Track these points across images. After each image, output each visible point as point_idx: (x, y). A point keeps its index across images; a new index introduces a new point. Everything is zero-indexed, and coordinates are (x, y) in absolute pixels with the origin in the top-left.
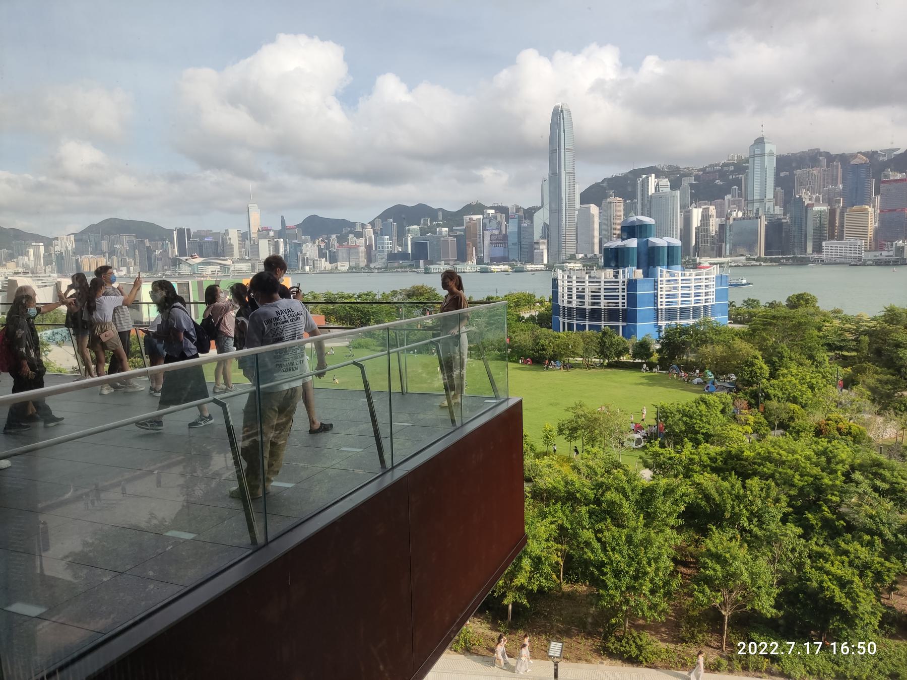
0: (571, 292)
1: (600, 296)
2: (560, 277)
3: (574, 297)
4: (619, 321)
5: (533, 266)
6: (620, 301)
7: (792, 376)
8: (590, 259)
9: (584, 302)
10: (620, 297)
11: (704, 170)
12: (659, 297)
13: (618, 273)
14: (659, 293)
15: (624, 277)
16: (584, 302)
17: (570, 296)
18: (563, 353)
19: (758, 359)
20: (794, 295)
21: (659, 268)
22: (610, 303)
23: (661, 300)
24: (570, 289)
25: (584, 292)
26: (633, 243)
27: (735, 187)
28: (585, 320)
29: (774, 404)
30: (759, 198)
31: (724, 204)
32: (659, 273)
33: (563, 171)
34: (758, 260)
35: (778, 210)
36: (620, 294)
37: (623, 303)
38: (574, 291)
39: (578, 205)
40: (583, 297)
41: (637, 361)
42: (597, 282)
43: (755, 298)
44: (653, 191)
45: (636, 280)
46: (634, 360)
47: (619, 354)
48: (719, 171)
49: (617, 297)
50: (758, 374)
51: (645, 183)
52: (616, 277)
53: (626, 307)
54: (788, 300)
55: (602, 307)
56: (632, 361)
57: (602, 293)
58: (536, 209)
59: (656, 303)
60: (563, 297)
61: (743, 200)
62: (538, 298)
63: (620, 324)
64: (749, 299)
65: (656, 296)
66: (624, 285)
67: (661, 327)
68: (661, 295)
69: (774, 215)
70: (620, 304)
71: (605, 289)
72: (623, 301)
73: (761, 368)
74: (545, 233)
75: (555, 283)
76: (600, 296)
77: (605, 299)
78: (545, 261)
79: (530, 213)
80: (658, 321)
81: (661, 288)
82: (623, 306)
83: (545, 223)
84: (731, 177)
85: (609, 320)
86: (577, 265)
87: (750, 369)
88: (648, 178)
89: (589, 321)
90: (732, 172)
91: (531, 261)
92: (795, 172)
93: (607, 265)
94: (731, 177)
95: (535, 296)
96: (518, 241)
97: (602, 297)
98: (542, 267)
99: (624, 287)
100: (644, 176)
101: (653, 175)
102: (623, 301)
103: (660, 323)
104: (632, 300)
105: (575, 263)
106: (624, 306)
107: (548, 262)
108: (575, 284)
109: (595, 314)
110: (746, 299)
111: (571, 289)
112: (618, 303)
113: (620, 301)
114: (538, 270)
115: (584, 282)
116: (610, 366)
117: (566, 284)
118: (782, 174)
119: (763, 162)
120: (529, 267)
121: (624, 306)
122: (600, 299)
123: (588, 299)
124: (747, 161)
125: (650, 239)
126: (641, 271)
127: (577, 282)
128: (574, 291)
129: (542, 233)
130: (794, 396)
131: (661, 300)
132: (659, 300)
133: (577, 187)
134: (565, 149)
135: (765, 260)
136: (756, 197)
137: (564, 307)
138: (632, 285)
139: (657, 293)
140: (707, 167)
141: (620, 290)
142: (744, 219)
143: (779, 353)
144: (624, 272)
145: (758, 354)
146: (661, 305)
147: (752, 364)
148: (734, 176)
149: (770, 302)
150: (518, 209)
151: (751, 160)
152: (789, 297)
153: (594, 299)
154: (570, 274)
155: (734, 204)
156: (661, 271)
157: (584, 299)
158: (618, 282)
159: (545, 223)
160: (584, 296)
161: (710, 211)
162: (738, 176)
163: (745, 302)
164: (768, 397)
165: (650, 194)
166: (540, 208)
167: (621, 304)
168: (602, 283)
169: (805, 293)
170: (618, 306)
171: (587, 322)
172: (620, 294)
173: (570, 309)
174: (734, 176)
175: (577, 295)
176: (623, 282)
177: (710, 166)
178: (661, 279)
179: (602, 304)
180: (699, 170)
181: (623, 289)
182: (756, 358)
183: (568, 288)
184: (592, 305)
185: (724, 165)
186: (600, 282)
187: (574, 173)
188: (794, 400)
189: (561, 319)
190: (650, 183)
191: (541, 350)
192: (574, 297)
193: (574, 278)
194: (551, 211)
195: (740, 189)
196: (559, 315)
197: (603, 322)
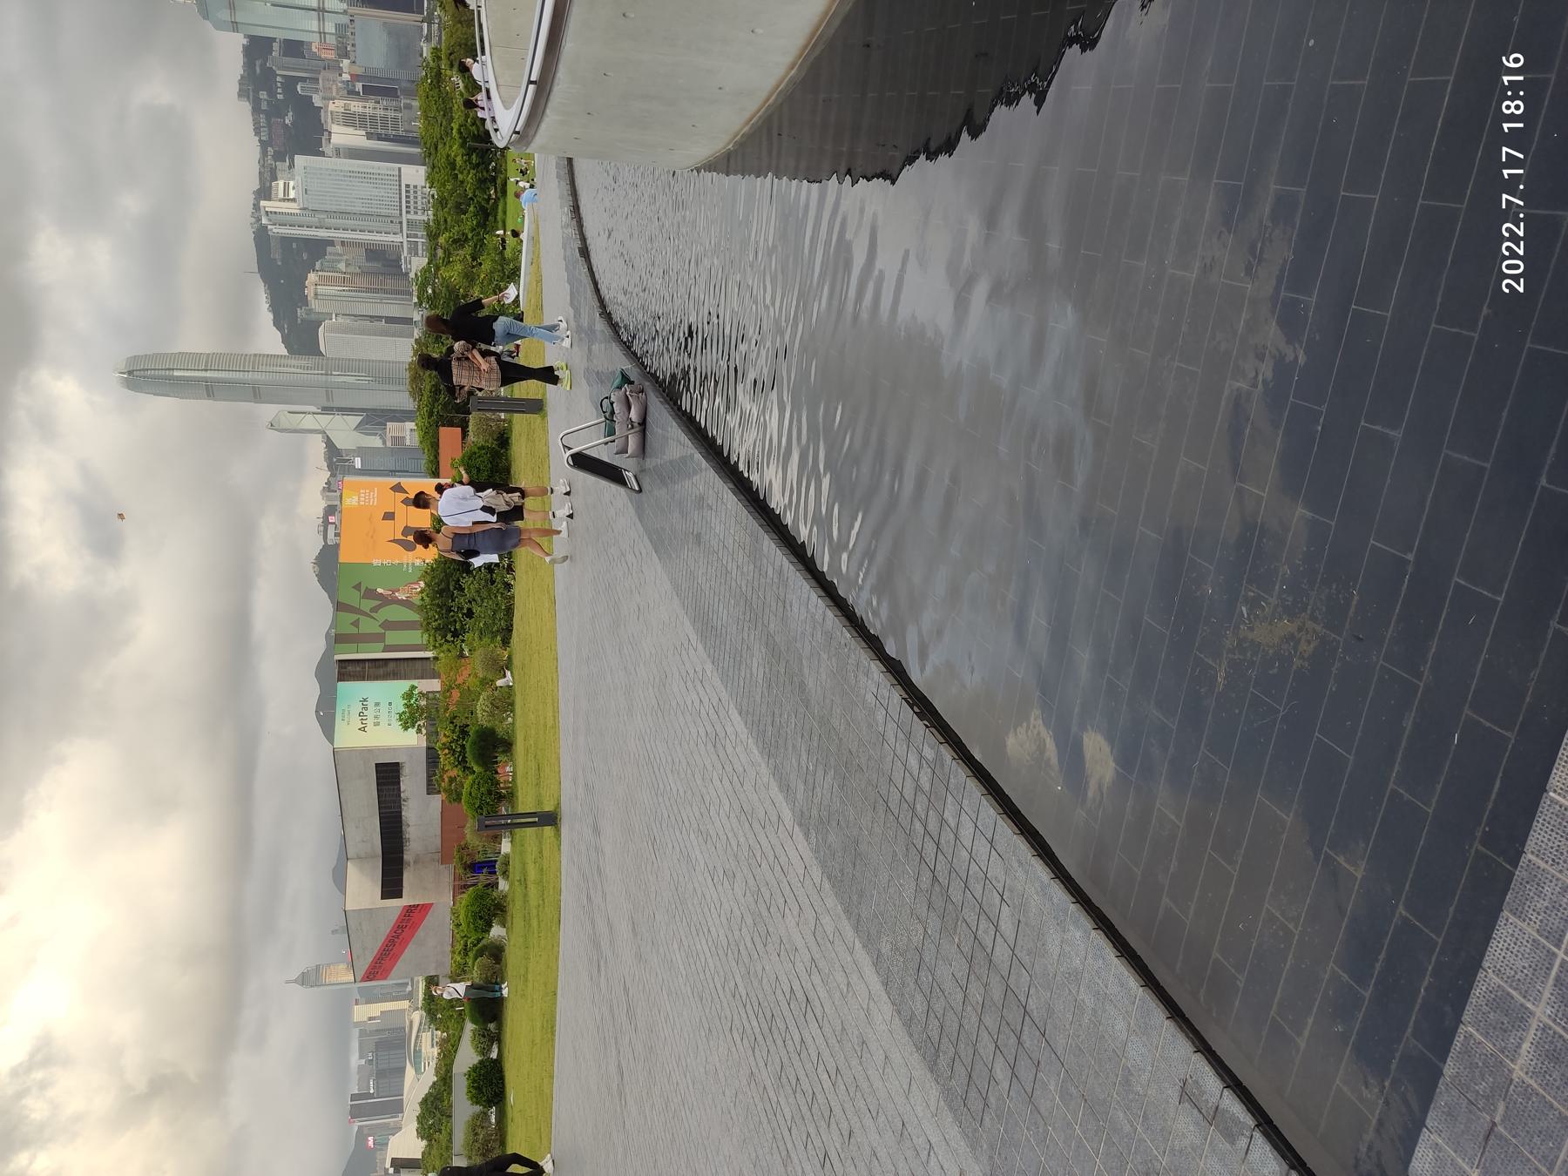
11: (264, 145)
74: (375, 429)
100: (264, 221)
134: (206, 370)
140: (260, 141)
161: (337, 110)
165: (298, 211)
177: (257, 131)
180: (264, 153)
185: (256, 110)
190: (277, 210)
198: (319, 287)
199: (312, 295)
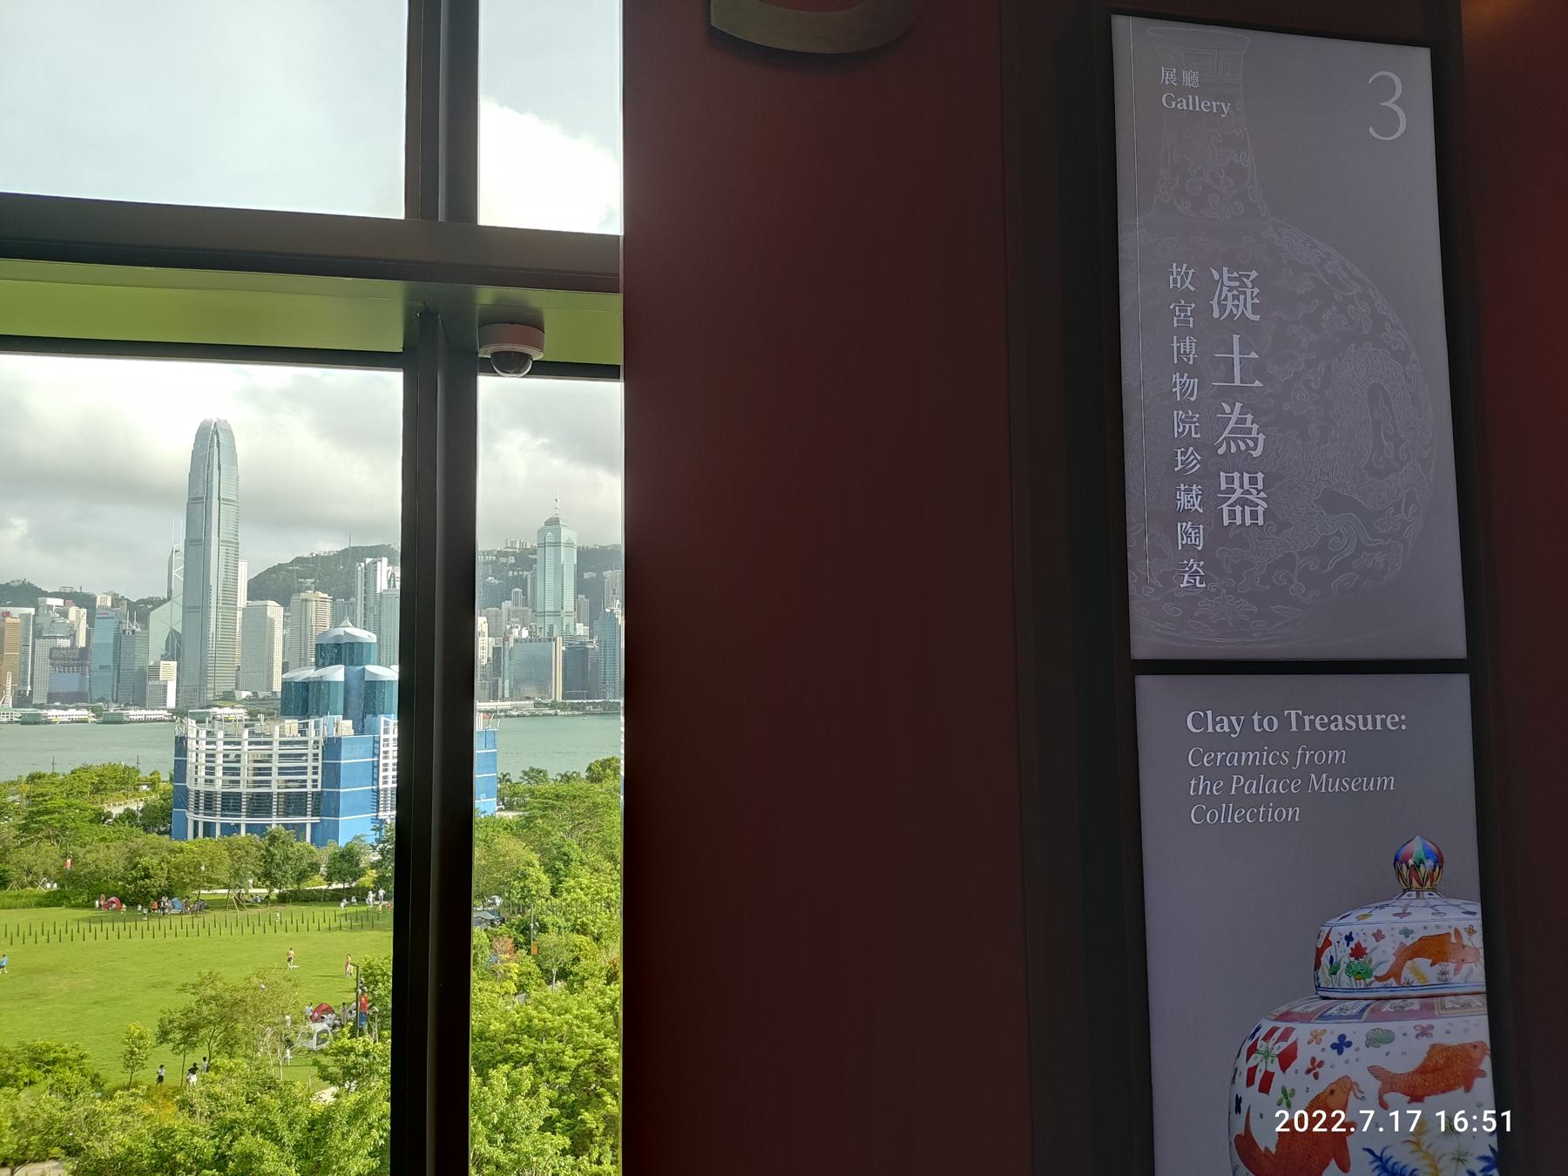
0: (213, 762)
1: (270, 769)
2: (192, 734)
3: (219, 773)
4: (305, 815)
5: (144, 712)
7: (582, 889)
8: (264, 699)
9: (238, 782)
10: (310, 771)
12: (381, 768)
13: (306, 725)
14: (382, 761)
15: (317, 734)
16: (238, 782)
17: (210, 771)
18: (188, 880)
19: (533, 866)
20: (597, 761)
21: (382, 718)
22: (289, 781)
23: (386, 774)
24: (211, 756)
25: (239, 761)
26: (337, 673)
27: (518, 589)
28: (240, 816)
29: (551, 938)
30: (552, 609)
31: (501, 615)
32: (382, 727)
33: (214, 537)
34: (553, 706)
35: (581, 630)
36: (310, 764)
37: (315, 781)
38: (220, 759)
39: (242, 599)
40: (236, 772)
41: (334, 886)
42: (266, 743)
43: (542, 768)
44: (385, 586)
45: (339, 739)
46: (330, 885)
47: (302, 876)
48: (492, 562)
49: (303, 770)
50: (533, 892)
51: (370, 574)
52: (302, 733)
53: (319, 789)
54: (589, 769)
55: (274, 789)
56: (324, 887)
57: (275, 764)
58: (157, 603)
59: (375, 780)
60: (196, 773)
61: (530, 610)
62: (145, 773)
63: (309, 820)
64: (532, 770)
65: (375, 766)
66: (318, 748)
67: (383, 821)
68: (385, 765)
69: (574, 637)
70: (309, 784)
71: (281, 756)
72: (315, 777)
73: (539, 881)
74: (173, 651)
75: (181, 744)
76: (270, 769)
77: (280, 774)
78: (171, 702)
79: (141, 610)
80: (378, 811)
81: (385, 752)
83: (173, 631)
84: (510, 573)
85: (287, 814)
86: (235, 711)
87: (522, 884)
88: (375, 563)
89: (247, 816)
90: (513, 567)
91: (141, 704)
92: (604, 573)
93: (286, 712)
94: (510, 573)
95: (138, 772)
96: (114, 662)
97: (275, 771)
98: (162, 714)
99: (316, 751)
100: (368, 560)
101: (385, 560)
102: (315, 777)
103: (382, 815)
104: (332, 774)
105: (233, 707)
107: (177, 705)
108: (221, 747)
109: (260, 804)
110: (527, 770)
111: (213, 756)
112: (305, 781)
113: (309, 777)
114: (155, 720)
115: (239, 743)
116: (282, 899)
117: (203, 746)
118: (586, 576)
119: (557, 556)
120: (135, 713)
122: (270, 775)
123: (245, 776)
124: (534, 552)
125: (369, 668)
126: (349, 723)
127: (225, 743)
128: (220, 759)
129: (167, 649)
130: (583, 922)
131: (386, 774)
132: (382, 774)
133: (243, 567)
135: (563, 707)
136: (549, 608)
137: (198, 793)
138: (332, 747)
139: (378, 761)
141: (310, 757)
142: (531, 641)
143: (565, 854)
144: (317, 726)
145: (535, 858)
146: (385, 783)
147: (525, 876)
148: (516, 573)
149: (563, 773)
150: (117, 600)
151: (540, 551)
152: (591, 764)
153: (260, 775)
154: (213, 727)
155: (517, 617)
156: (386, 723)
157: (238, 775)
158: (306, 742)
159: (173, 631)
160: (239, 769)
162: (521, 573)
163: (525, 773)
164: (543, 928)
165: (378, 591)
166: (162, 602)
167: (312, 783)
168: (276, 744)
169: (613, 758)
170: (305, 787)
171: (243, 818)
172: (310, 764)
173: (209, 796)
174: (516, 573)
175: (224, 768)
176: (316, 742)
178: (386, 736)
179: (274, 785)
181: (316, 755)
182: (529, 864)
183: (207, 755)
184: (254, 787)
185: (500, 554)
186: (270, 743)
187: (237, 544)
188: (582, 930)
189: (191, 816)
190: (379, 572)
191: (142, 879)
192: (219, 773)
193: (221, 735)
194: (187, 609)
195: (525, 593)
196: (187, 808)
197: (274, 818)
198: (314, 603)
199: (305, 597)
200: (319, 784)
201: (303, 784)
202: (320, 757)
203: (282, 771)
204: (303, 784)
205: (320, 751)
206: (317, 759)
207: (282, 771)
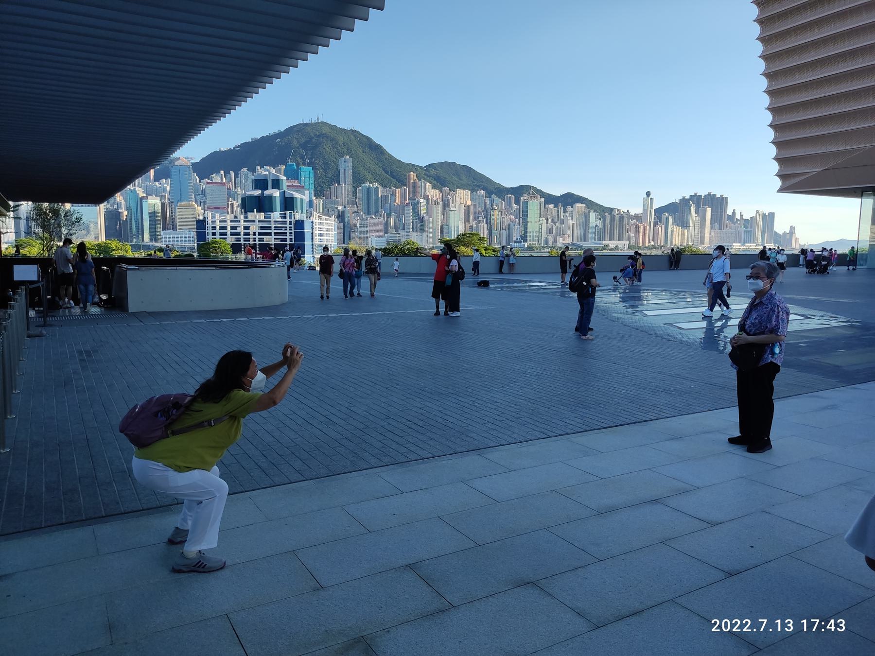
6: (288, 237)
10: (288, 234)
15: (290, 218)
36: (288, 231)
49: (285, 234)
53: (293, 242)
57: (273, 231)
70: (288, 240)
72: (291, 237)
82: (290, 241)
97: (273, 234)
102: (291, 237)
104: (299, 236)
106: (292, 241)
121: (292, 241)
122: (271, 235)
170: (286, 241)
176: (290, 222)
181: (290, 227)
200: (293, 240)
201: (285, 240)
202: (293, 228)
203: (276, 234)
204: (285, 240)
205: (292, 226)
206: (292, 230)
207: (276, 234)
